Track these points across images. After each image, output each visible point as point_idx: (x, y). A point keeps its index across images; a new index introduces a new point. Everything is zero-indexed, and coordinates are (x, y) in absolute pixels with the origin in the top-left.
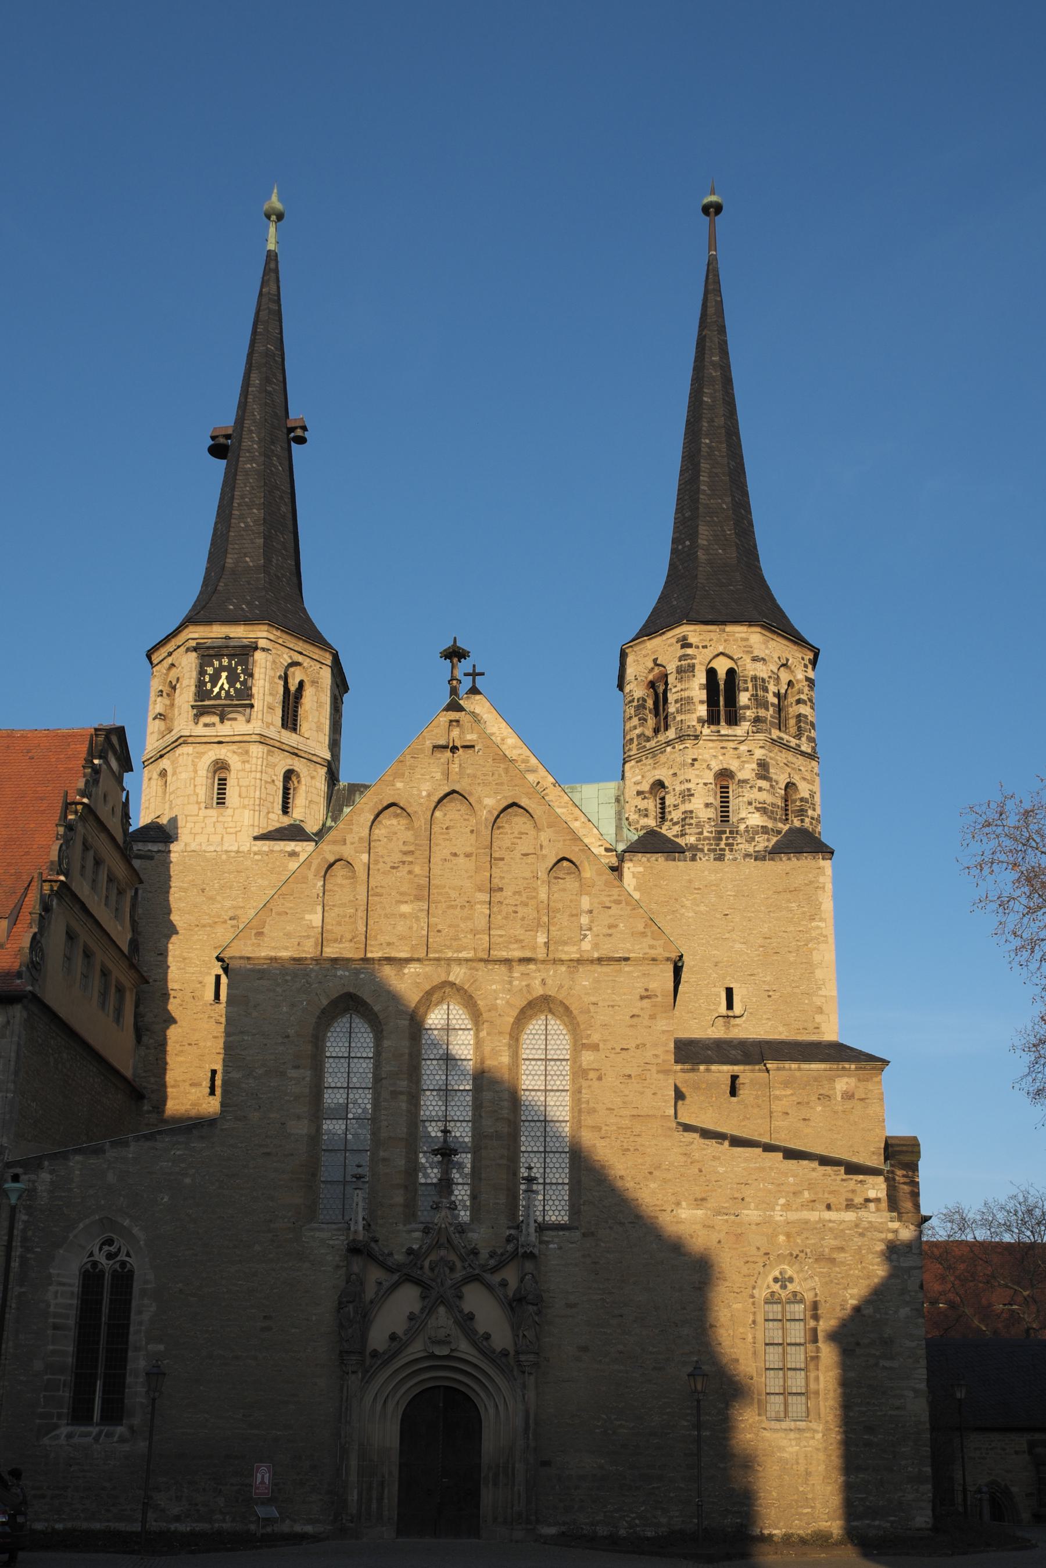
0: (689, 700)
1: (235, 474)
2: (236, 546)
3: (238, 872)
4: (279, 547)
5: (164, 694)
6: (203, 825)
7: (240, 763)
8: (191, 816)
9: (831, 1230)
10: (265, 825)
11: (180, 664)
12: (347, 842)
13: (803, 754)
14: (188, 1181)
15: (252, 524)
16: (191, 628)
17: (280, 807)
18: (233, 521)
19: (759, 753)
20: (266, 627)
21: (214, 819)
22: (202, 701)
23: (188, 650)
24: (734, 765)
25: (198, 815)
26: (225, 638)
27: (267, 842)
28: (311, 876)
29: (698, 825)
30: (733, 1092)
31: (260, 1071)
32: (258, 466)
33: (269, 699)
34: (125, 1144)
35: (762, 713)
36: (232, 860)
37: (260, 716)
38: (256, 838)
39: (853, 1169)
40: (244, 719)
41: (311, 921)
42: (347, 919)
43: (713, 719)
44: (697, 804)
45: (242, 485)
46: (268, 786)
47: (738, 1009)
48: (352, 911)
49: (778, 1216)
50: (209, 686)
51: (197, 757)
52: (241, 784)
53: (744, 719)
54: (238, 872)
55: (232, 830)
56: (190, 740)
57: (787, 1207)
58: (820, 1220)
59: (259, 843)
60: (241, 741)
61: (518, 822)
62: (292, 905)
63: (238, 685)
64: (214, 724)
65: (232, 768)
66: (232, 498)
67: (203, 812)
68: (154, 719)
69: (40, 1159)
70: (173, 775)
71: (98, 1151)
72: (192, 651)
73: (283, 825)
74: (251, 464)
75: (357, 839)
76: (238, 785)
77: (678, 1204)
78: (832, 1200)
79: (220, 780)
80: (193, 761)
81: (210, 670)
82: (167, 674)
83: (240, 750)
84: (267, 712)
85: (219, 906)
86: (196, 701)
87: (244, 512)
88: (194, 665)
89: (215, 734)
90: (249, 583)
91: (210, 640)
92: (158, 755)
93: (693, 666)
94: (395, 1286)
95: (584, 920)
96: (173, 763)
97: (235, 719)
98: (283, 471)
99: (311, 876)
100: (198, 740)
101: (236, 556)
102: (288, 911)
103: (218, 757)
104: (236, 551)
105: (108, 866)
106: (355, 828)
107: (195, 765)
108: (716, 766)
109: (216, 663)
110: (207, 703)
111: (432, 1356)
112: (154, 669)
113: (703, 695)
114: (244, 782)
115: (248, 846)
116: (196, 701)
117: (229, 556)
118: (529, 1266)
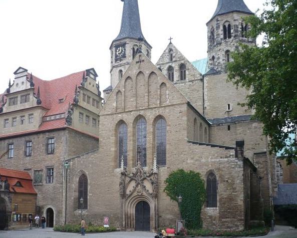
0: (219, 34)
9: (221, 163)
13: (249, 42)
14: (94, 162)
19: (235, 45)
24: (229, 48)
29: (221, 65)
30: (229, 129)
31: (106, 138)
34: (83, 155)
35: (236, 34)
39: (227, 148)
43: (225, 38)
44: (221, 60)
47: (231, 109)
49: (209, 160)
53: (232, 36)
57: (211, 159)
58: (220, 161)
60: (124, 65)
61: (153, 76)
69: (70, 159)
71: (79, 157)
77: (187, 160)
78: (222, 156)
93: (219, 26)
94: (131, 181)
95: (167, 96)
108: (225, 50)
111: (138, 195)
113: (222, 32)
118: (156, 176)
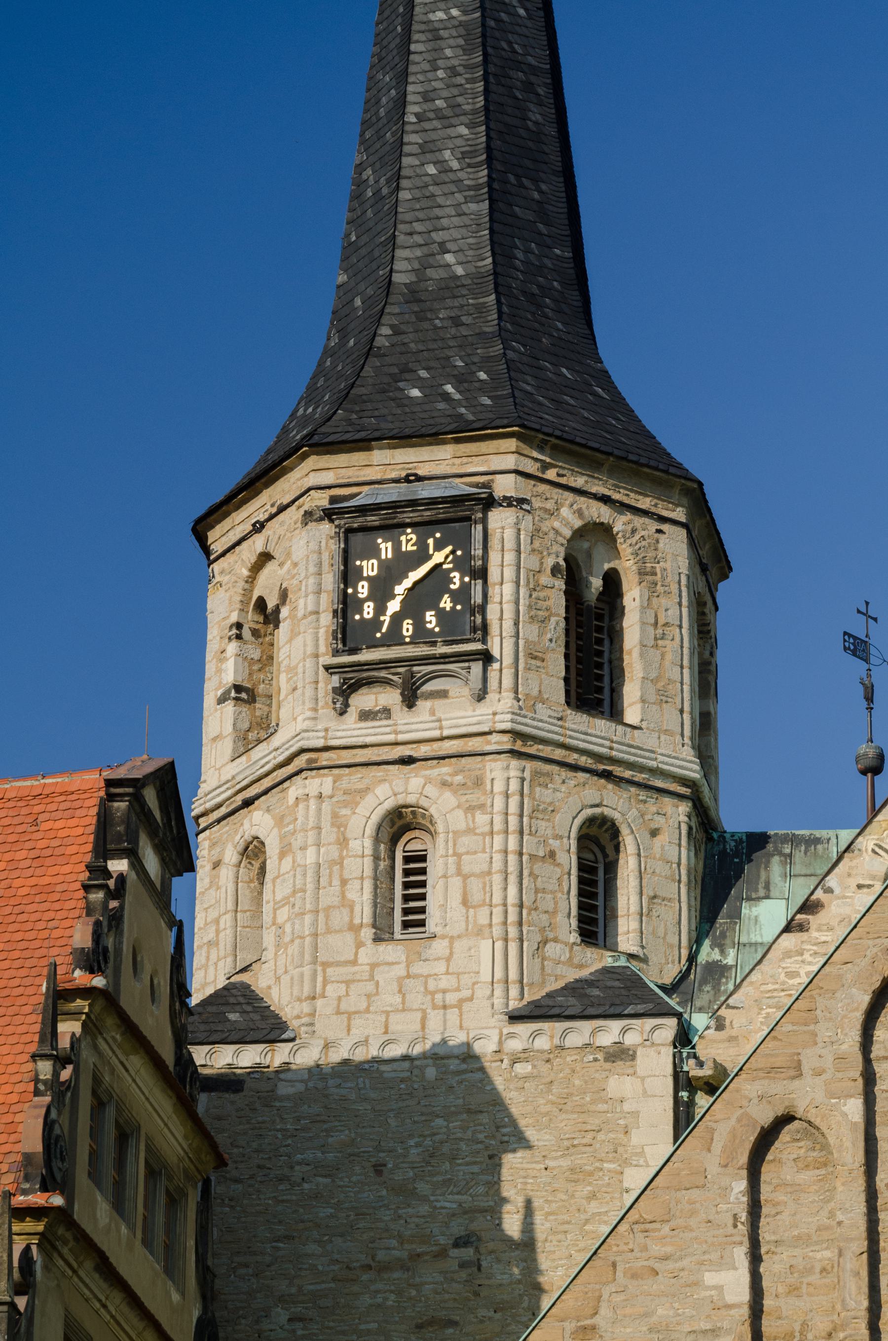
1: (407, 38)
2: (418, 227)
3: (469, 1111)
4: (530, 216)
5: (246, 633)
6: (370, 987)
7: (460, 813)
8: (338, 964)
10: (537, 978)
11: (289, 555)
12: (805, 1068)
15: (455, 165)
16: (313, 461)
17: (574, 922)
18: (406, 161)
20: (512, 444)
21: (400, 971)
22: (354, 651)
23: (308, 516)
25: (354, 962)
26: (407, 479)
27: (545, 1026)
28: (713, 1168)
32: (465, 13)
33: (528, 631)
36: (453, 1081)
37: (508, 682)
38: (515, 1018)
40: (466, 691)
41: (719, 1288)
42: (815, 1278)
45: (426, 66)
46: (538, 867)
48: (827, 1254)
50: (369, 610)
51: (345, 804)
52: (466, 869)
54: (469, 1111)
55: (451, 998)
56: (325, 758)
59: (524, 1029)
62: (669, 1249)
63: (446, 603)
64: (386, 712)
65: (440, 828)
66: (401, 103)
67: (369, 953)
68: (221, 700)
70: (282, 855)
72: (321, 519)
73: (585, 973)
74: (446, 11)
75: (830, 1058)
76: (459, 872)
79: (407, 860)
80: (335, 816)
81: (370, 568)
82: (251, 580)
83: (459, 778)
84: (528, 669)
85: (424, 1209)
86: (336, 653)
87: (433, 136)
88: (326, 556)
89: (391, 738)
90: (456, 322)
91: (365, 489)
92: (239, 800)
96: (280, 821)
97: (443, 694)
98: (530, 17)
99: (713, 1168)
100: (347, 757)
101: (418, 253)
102: (657, 1266)
103: (401, 800)
104: (418, 239)
105: (148, 1137)
106: (824, 1031)
107: (338, 823)
109: (386, 549)
110: (366, 656)
112: (216, 567)
114: (475, 863)
115: (496, 1039)
116: (336, 653)
117: (399, 253)
